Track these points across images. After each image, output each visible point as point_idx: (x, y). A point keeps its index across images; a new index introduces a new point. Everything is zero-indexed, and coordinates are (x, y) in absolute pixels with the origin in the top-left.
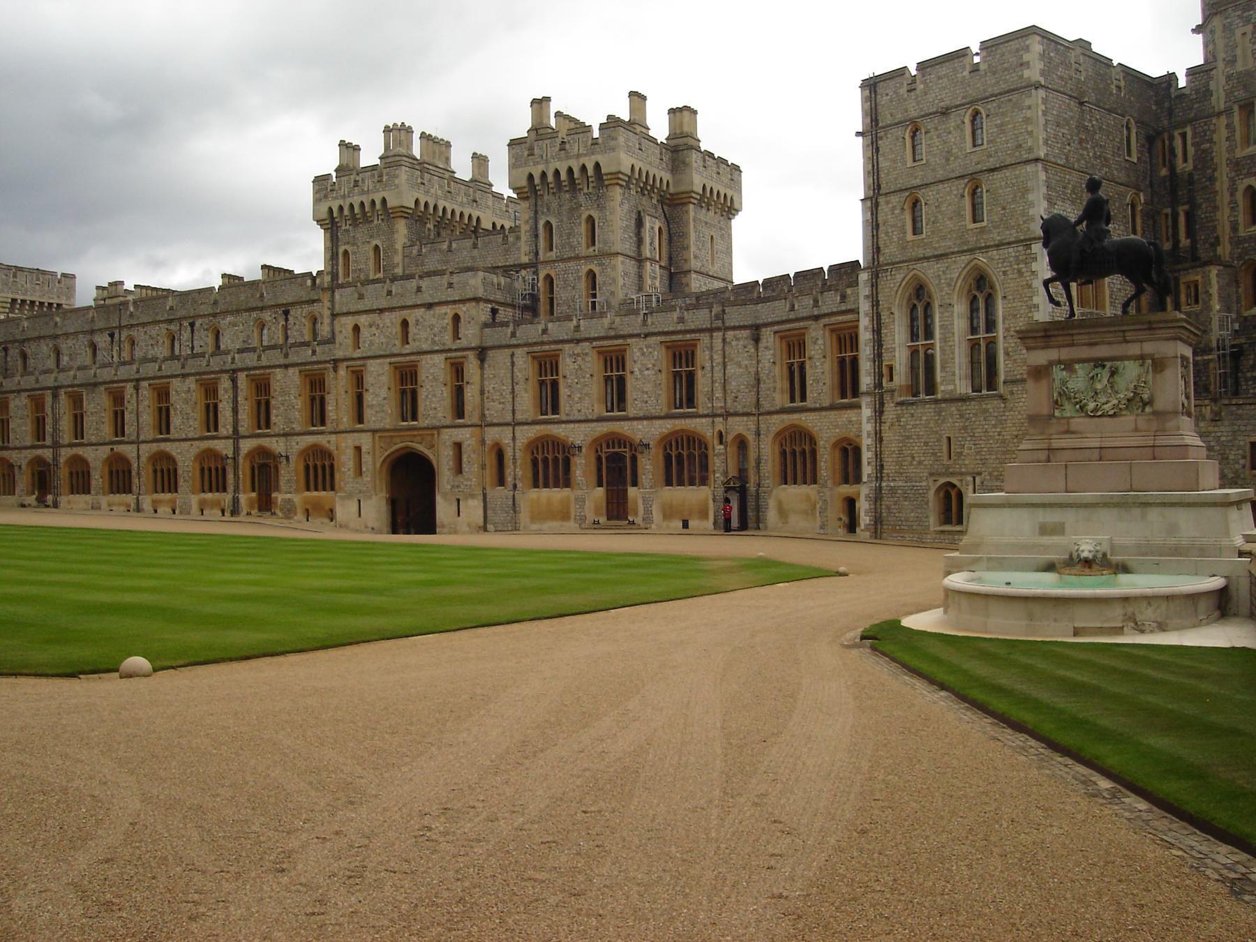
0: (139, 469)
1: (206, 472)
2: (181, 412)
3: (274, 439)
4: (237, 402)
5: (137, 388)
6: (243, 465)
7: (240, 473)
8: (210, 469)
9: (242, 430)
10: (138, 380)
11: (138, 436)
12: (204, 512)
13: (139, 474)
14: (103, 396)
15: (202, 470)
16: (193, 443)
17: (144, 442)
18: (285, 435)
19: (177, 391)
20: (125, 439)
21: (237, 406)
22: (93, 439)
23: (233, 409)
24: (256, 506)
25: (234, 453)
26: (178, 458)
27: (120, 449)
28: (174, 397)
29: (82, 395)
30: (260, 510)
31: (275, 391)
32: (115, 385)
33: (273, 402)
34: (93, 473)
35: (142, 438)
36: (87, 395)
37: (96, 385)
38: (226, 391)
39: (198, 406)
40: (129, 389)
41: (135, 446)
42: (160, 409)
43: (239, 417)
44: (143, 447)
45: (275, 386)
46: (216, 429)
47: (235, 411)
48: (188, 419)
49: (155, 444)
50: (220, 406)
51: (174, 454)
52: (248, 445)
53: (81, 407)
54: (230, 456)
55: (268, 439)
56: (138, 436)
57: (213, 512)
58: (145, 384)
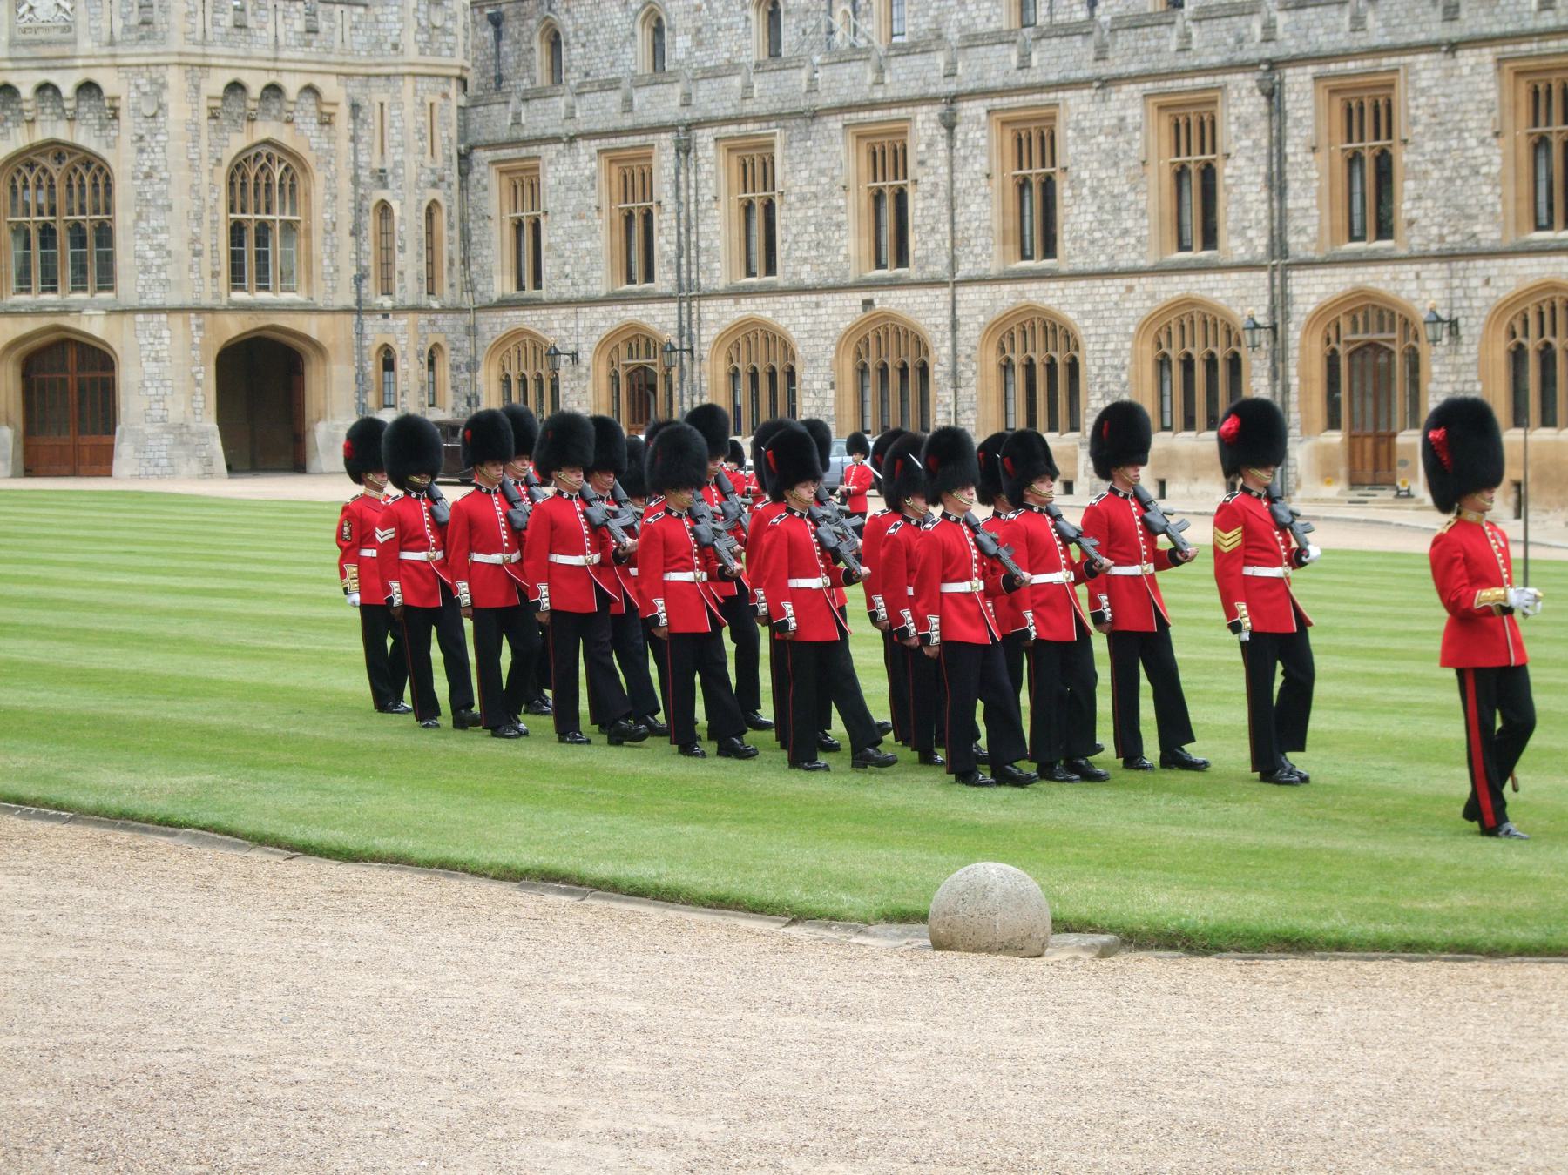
0: (955, 364)
1: (1177, 370)
2: (1094, 192)
3: (1409, 270)
4: (1282, 157)
5: (949, 124)
6: (1302, 348)
7: (1293, 371)
8: (1188, 364)
9: (1298, 244)
10: (953, 99)
11: (953, 263)
12: (1169, 490)
13: (955, 375)
14: (840, 148)
15: (1163, 363)
16: (1133, 281)
17: (969, 281)
18: (1448, 257)
19: (1080, 130)
20: (911, 272)
21: (1281, 173)
22: (808, 276)
23: (1269, 178)
24: (1343, 471)
25: (1272, 311)
26: (1085, 329)
27: (888, 301)
28: (1069, 147)
29: (772, 145)
30: (1354, 483)
31: (1414, 122)
32: (877, 115)
33: (1403, 158)
34: (804, 374)
35: (965, 269)
36: (789, 144)
37: (815, 115)
38: (1246, 126)
39: (1152, 170)
40: (924, 125)
41: (943, 293)
42: (1023, 185)
43: (1290, 204)
44: (968, 295)
45: (1413, 109)
46: (1210, 238)
47: (1277, 185)
48: (1117, 210)
49: (1006, 288)
50: (1225, 172)
51: (1071, 316)
52: (1321, 289)
53: (769, 181)
54: (1260, 320)
55: (1386, 271)
56: (953, 263)
57: (1198, 488)
58: (972, 110)
